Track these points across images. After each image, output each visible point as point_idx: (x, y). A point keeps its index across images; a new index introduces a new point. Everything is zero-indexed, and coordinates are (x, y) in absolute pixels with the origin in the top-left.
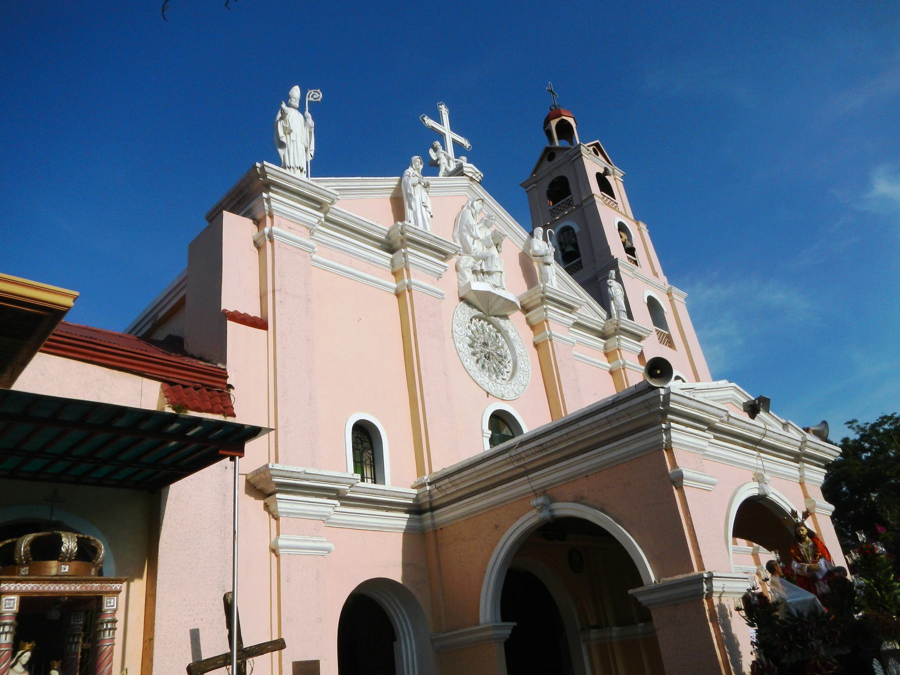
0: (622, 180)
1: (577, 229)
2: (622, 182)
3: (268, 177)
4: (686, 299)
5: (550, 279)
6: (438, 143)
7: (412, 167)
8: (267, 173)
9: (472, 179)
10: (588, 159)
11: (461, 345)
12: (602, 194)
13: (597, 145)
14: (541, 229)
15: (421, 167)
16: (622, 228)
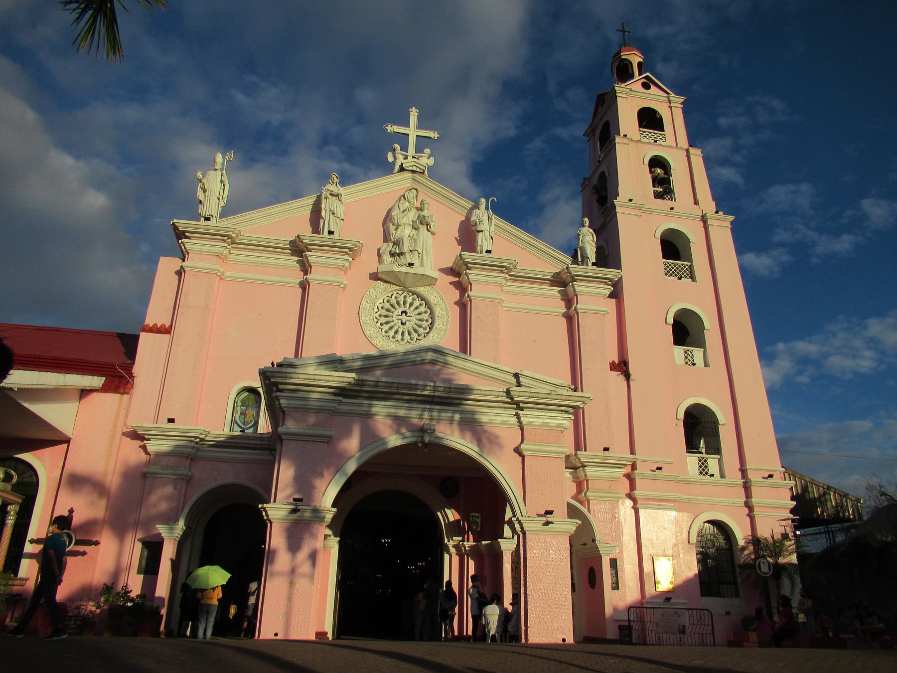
0: (682, 106)
1: (607, 175)
2: (682, 108)
3: (180, 229)
4: (731, 223)
5: (480, 243)
6: (397, 146)
7: (330, 183)
8: (178, 227)
9: (413, 172)
10: (627, 98)
11: (367, 319)
13: (647, 78)
14: (483, 200)
15: (338, 180)
16: (657, 162)
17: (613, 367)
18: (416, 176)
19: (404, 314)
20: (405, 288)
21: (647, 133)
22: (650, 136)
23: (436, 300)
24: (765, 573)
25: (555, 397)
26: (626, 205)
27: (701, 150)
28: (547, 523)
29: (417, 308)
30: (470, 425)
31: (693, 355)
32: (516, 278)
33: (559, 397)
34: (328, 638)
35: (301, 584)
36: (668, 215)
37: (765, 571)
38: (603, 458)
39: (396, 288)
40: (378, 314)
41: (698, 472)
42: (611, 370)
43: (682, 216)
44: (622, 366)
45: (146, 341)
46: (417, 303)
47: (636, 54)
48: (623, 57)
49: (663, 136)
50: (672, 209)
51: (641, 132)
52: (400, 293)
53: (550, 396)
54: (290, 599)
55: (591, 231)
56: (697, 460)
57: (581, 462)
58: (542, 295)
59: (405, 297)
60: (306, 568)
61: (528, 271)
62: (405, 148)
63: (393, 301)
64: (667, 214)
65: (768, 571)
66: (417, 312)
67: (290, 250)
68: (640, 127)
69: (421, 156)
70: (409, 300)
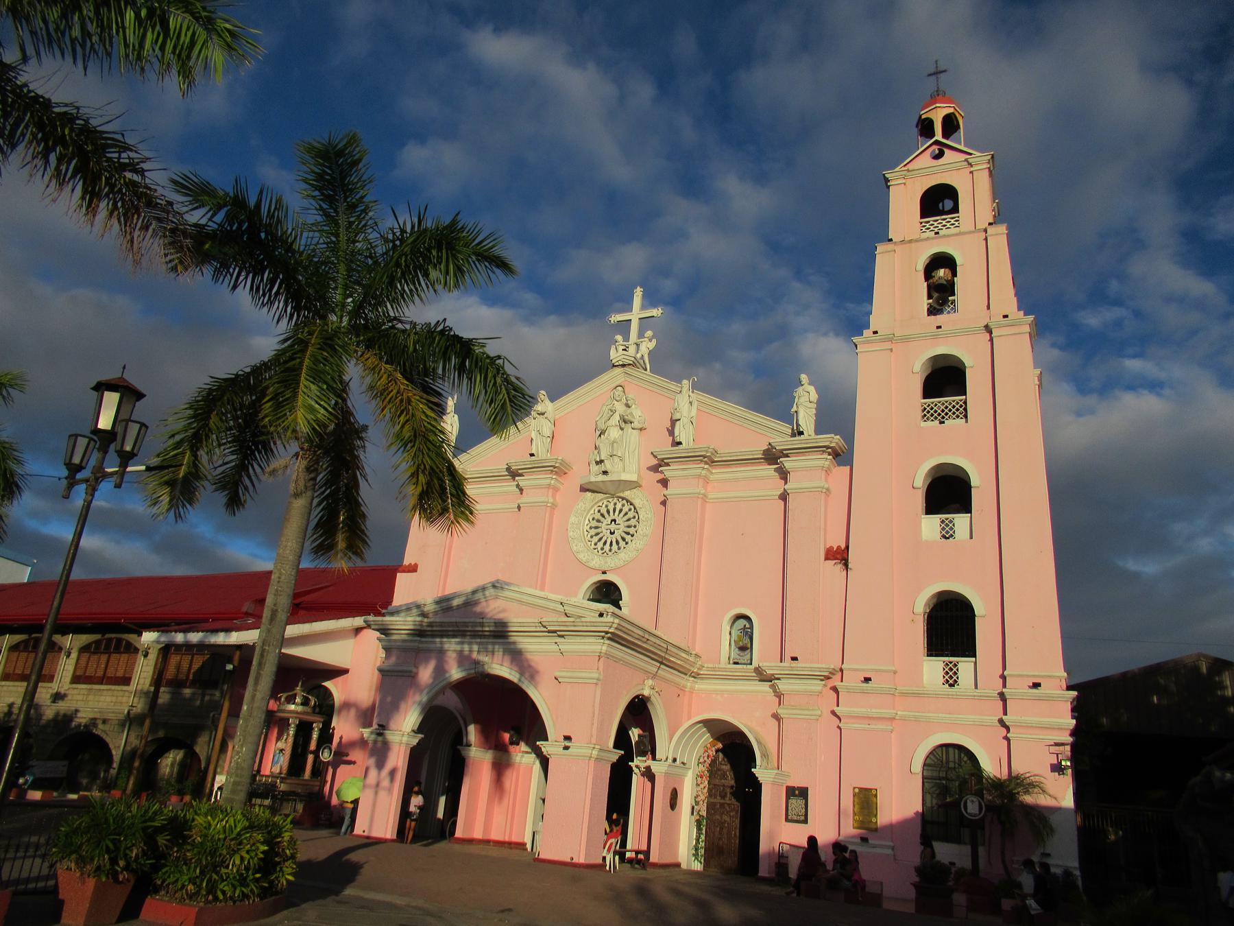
6: (619, 338)
9: (623, 366)
10: (905, 184)
12: (921, 223)
14: (685, 382)
17: (832, 554)
18: (627, 369)
19: (613, 523)
20: (613, 496)
21: (931, 223)
22: (936, 225)
23: (641, 503)
24: (970, 814)
25: (581, 624)
26: (871, 340)
27: (1006, 224)
28: (566, 748)
29: (626, 514)
30: (516, 656)
31: (954, 525)
32: (727, 463)
33: (585, 624)
34: (527, 849)
35: (383, 794)
36: (935, 337)
37: (973, 812)
38: (790, 668)
39: (602, 496)
40: (589, 526)
41: (942, 680)
42: (827, 558)
43: (955, 333)
44: (840, 556)
45: (401, 578)
46: (626, 509)
47: (939, 107)
48: (923, 117)
49: (957, 219)
50: (939, 327)
51: (923, 224)
52: (610, 500)
53: (575, 624)
54: (374, 805)
55: (812, 389)
56: (942, 665)
57: (767, 675)
58: (757, 478)
59: (615, 504)
60: (386, 783)
61: (735, 454)
62: (627, 339)
63: (604, 511)
64: (934, 335)
65: (978, 812)
66: (626, 518)
67: (510, 476)
68: (921, 218)
69: (642, 342)
70: (619, 507)
